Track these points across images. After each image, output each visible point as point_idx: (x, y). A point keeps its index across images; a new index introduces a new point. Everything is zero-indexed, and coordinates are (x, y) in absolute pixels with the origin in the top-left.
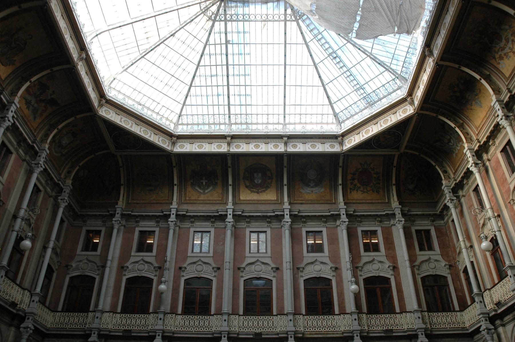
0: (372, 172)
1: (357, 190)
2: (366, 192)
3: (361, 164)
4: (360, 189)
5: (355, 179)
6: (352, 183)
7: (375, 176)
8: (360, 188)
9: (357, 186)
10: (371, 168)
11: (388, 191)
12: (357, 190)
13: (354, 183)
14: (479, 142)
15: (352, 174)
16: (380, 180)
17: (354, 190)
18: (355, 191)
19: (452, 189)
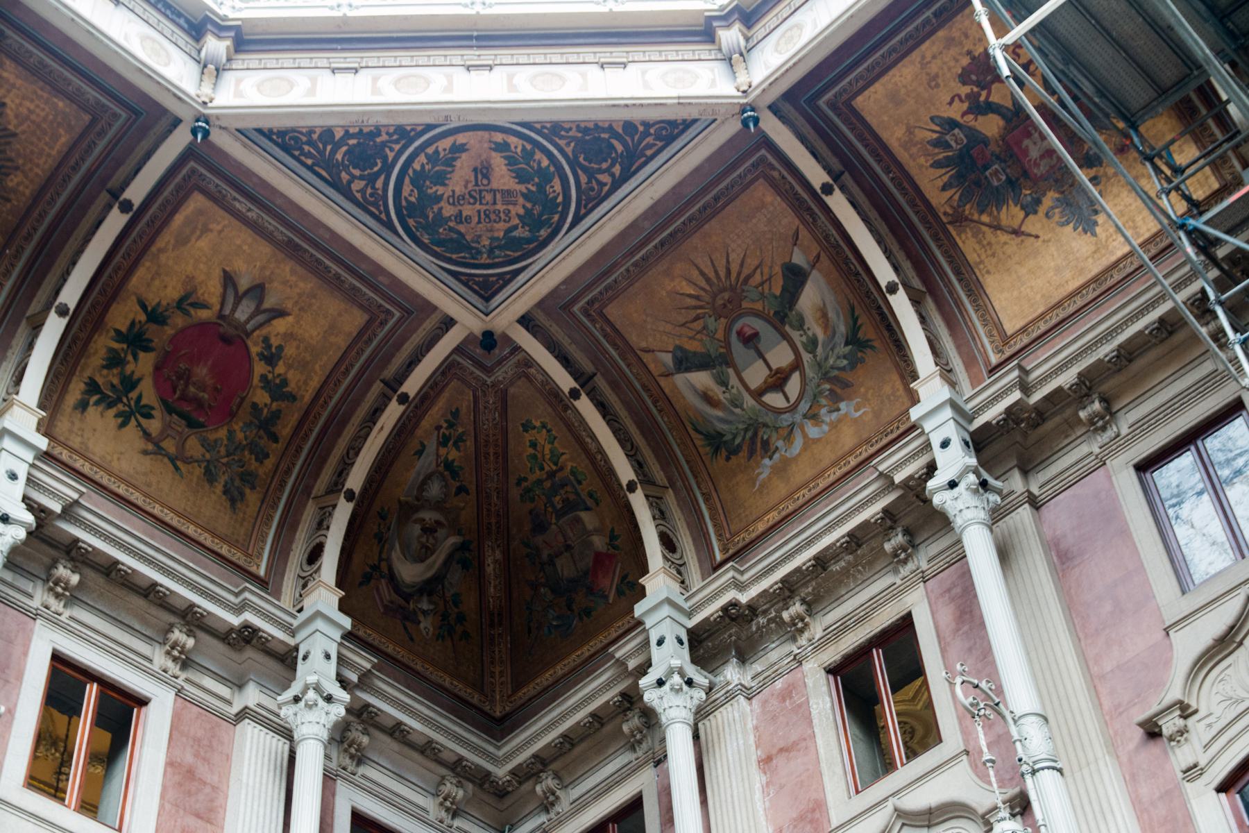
0: (260, 368)
1: (124, 419)
2: (167, 455)
3: (228, 279)
4: (143, 421)
5: (147, 349)
6: (114, 361)
7: (261, 397)
8: (148, 416)
9: (133, 395)
10: (266, 340)
11: (288, 526)
12: (124, 419)
13: (129, 368)
14: (1026, 389)
15: (143, 306)
16: (274, 438)
17: (110, 406)
18: (112, 412)
19: (690, 632)
